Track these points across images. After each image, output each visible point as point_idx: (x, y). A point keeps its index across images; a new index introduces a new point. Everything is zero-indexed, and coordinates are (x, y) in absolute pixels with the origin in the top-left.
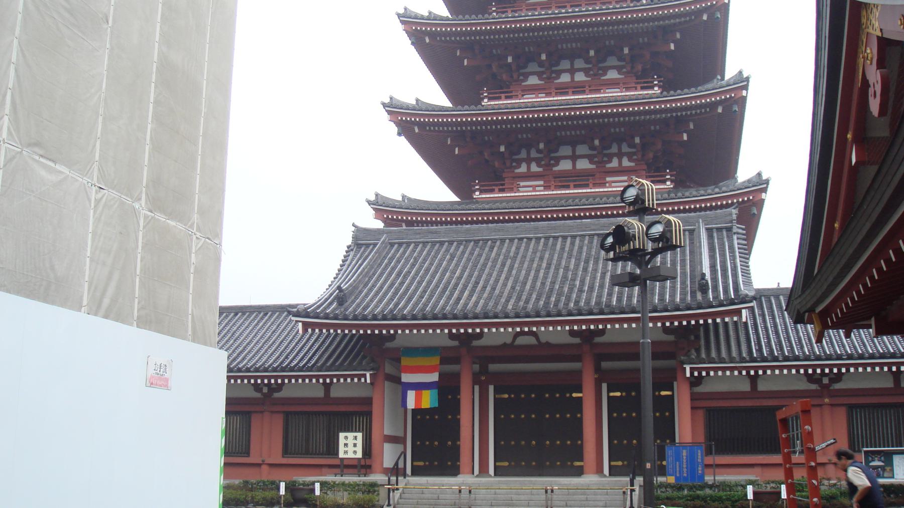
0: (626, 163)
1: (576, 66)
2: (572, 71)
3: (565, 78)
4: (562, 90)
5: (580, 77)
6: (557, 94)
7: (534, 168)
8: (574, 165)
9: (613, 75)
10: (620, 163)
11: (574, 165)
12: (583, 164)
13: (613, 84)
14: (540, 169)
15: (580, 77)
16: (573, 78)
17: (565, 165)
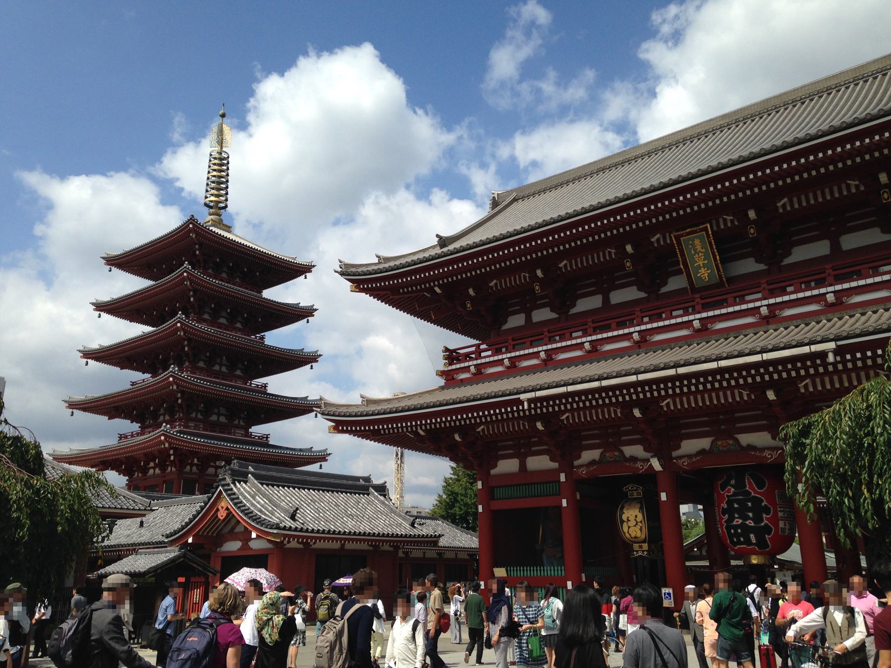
0: (242, 423)
2: (221, 365)
3: (217, 368)
5: (224, 369)
6: (215, 378)
7: (199, 416)
9: (238, 372)
12: (223, 419)
15: (224, 369)
17: (214, 418)
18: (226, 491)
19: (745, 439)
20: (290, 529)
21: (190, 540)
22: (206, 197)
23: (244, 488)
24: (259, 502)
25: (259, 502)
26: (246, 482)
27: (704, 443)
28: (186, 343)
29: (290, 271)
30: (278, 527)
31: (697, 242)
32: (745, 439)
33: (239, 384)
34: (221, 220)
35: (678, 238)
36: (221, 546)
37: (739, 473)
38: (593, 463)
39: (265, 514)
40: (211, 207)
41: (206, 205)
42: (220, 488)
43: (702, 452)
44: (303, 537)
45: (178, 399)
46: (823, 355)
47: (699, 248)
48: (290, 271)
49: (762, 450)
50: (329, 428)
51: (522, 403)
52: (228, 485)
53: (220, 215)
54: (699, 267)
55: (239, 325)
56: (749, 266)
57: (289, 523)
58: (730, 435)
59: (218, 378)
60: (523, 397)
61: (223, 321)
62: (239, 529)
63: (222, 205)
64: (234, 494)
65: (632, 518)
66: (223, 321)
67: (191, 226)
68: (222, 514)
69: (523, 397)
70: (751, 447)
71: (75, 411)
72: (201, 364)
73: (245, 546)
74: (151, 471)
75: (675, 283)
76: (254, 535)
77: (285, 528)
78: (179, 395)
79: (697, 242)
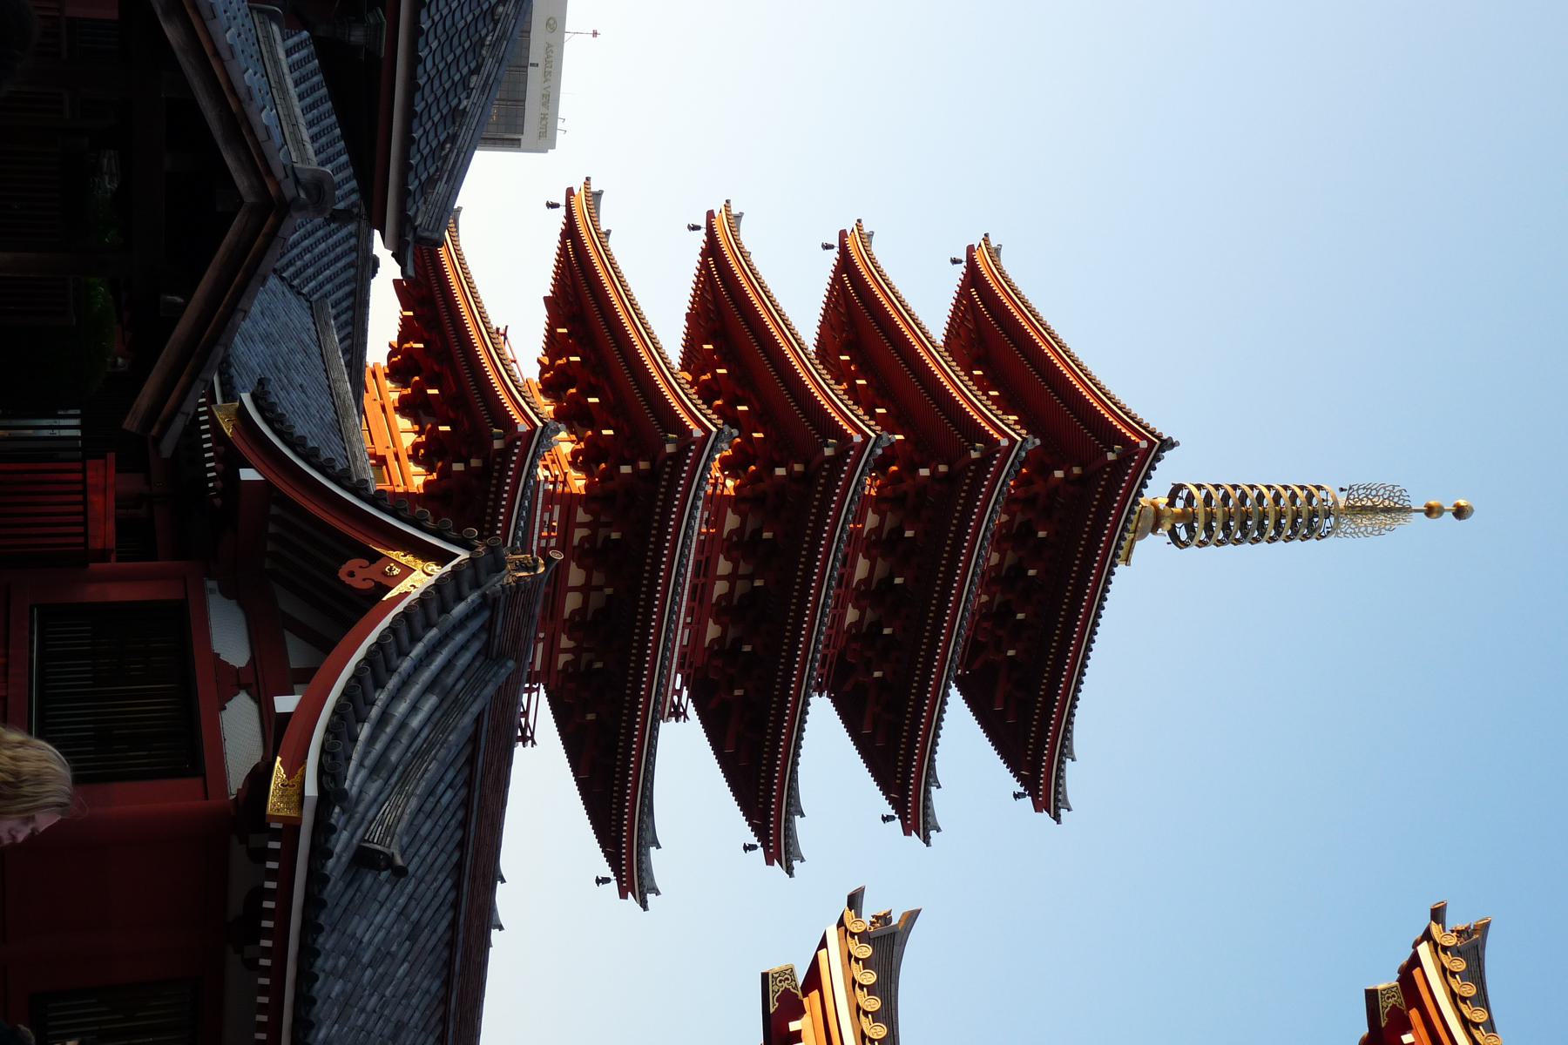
0: (563, 659)
1: (739, 584)
2: (731, 578)
3: (724, 567)
4: (705, 568)
6: (697, 564)
7: (579, 534)
8: (574, 589)
9: (712, 631)
10: (566, 651)
11: (574, 589)
12: (572, 602)
13: (697, 632)
14: (576, 541)
15: (720, 588)
16: (722, 578)
18: (455, 572)
20: (320, 851)
21: (247, 474)
22: (1199, 487)
23: (463, 647)
24: (414, 708)
25: (414, 708)
26: (485, 652)
28: (798, 467)
29: (1034, 751)
30: (331, 793)
33: (682, 637)
34: (1143, 536)
36: (227, 593)
39: (372, 739)
40: (1171, 504)
41: (1177, 489)
42: (464, 555)
44: (283, 914)
45: (632, 462)
48: (1034, 751)
50: (789, 973)
52: (476, 585)
53: (1154, 531)
55: (851, 615)
57: (341, 842)
59: (696, 574)
61: (862, 568)
62: (297, 654)
63: (1183, 536)
64: (445, 609)
66: (862, 568)
67: (1144, 444)
68: (355, 573)
71: (562, 211)
72: (731, 521)
73: (232, 682)
74: (404, 423)
76: (285, 704)
77: (323, 828)
78: (643, 465)
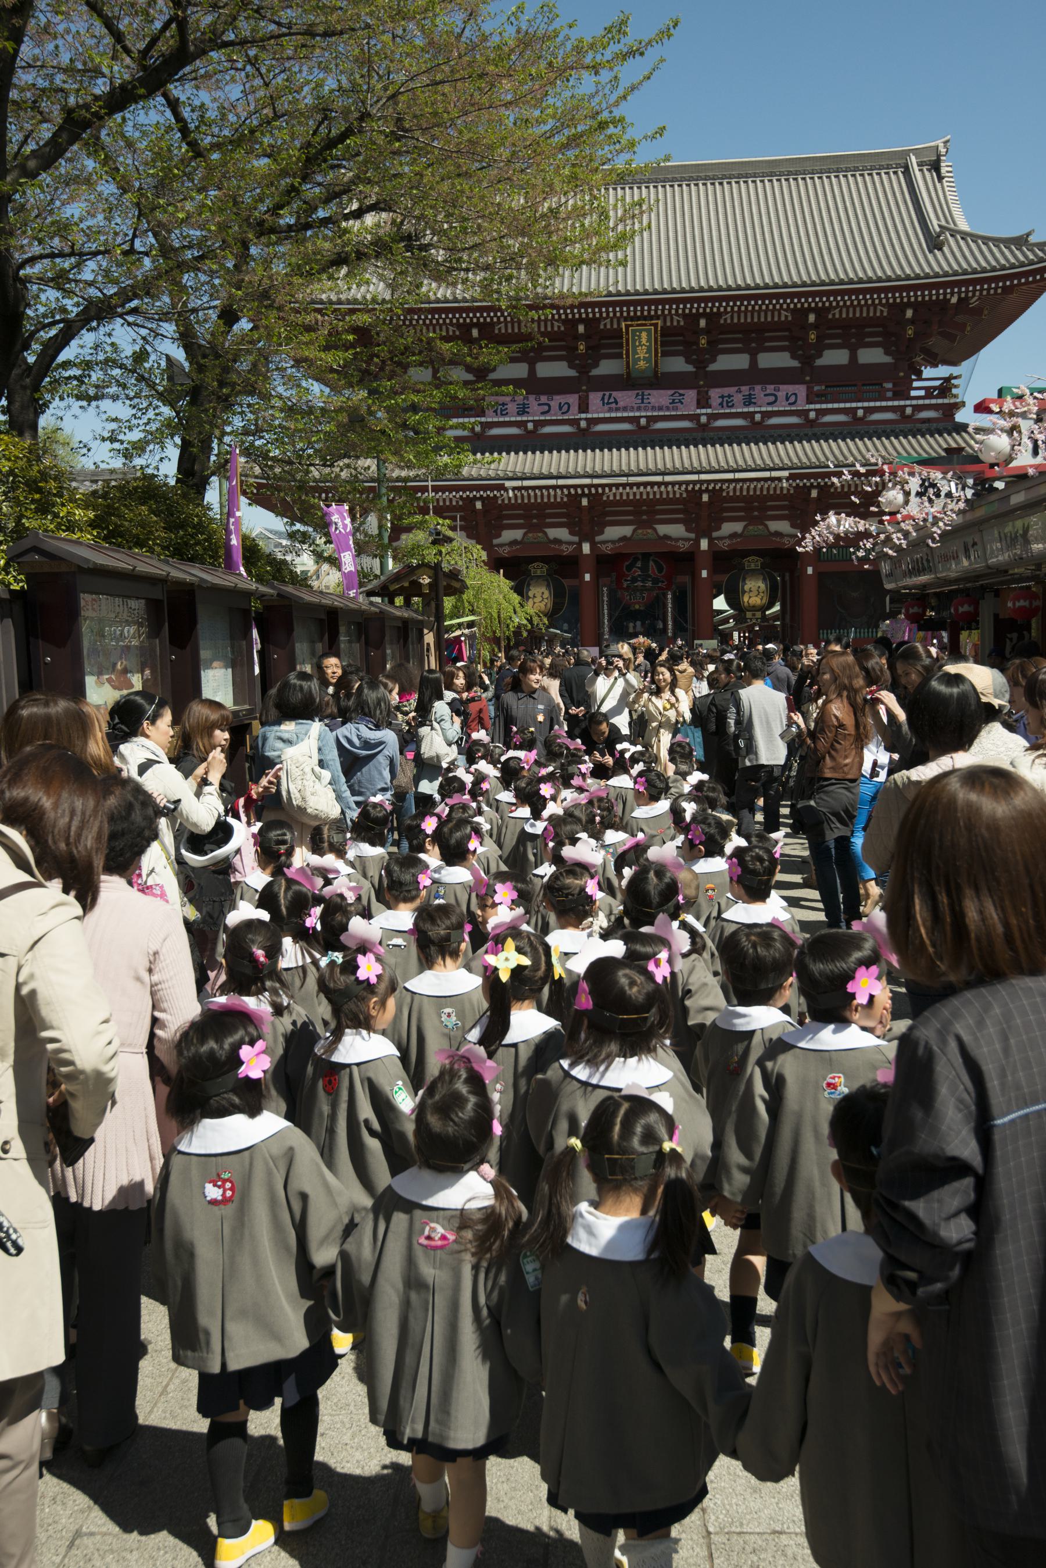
19: (663, 529)
27: (627, 531)
31: (644, 335)
32: (663, 529)
35: (627, 327)
37: (646, 556)
38: (514, 542)
43: (623, 539)
46: (779, 479)
47: (644, 341)
49: (677, 540)
51: (506, 490)
54: (639, 359)
56: (678, 364)
58: (649, 524)
60: (508, 484)
65: (538, 595)
69: (508, 484)
70: (667, 537)
75: (607, 367)
79: (644, 335)
